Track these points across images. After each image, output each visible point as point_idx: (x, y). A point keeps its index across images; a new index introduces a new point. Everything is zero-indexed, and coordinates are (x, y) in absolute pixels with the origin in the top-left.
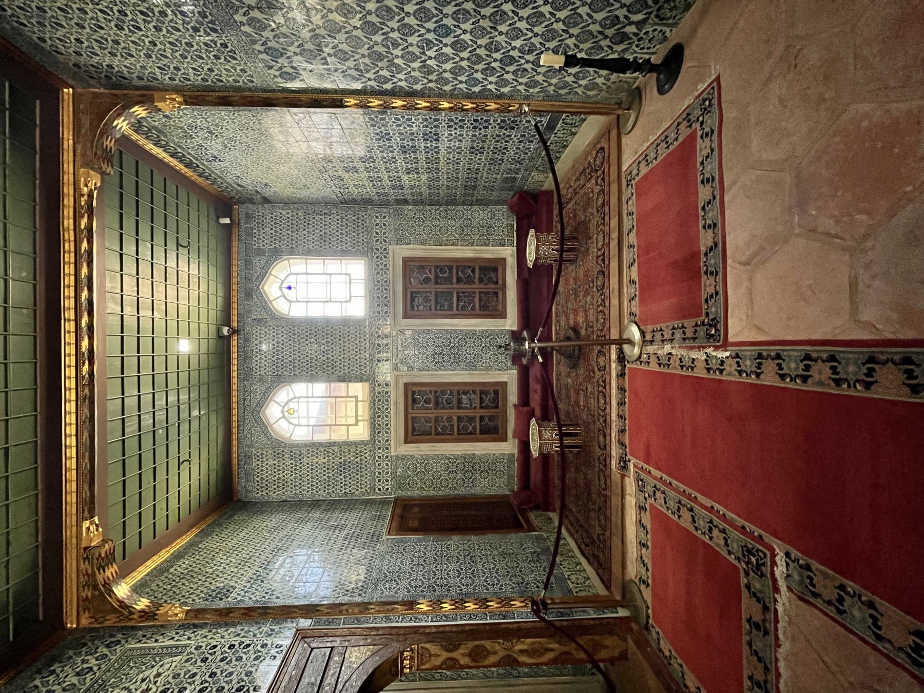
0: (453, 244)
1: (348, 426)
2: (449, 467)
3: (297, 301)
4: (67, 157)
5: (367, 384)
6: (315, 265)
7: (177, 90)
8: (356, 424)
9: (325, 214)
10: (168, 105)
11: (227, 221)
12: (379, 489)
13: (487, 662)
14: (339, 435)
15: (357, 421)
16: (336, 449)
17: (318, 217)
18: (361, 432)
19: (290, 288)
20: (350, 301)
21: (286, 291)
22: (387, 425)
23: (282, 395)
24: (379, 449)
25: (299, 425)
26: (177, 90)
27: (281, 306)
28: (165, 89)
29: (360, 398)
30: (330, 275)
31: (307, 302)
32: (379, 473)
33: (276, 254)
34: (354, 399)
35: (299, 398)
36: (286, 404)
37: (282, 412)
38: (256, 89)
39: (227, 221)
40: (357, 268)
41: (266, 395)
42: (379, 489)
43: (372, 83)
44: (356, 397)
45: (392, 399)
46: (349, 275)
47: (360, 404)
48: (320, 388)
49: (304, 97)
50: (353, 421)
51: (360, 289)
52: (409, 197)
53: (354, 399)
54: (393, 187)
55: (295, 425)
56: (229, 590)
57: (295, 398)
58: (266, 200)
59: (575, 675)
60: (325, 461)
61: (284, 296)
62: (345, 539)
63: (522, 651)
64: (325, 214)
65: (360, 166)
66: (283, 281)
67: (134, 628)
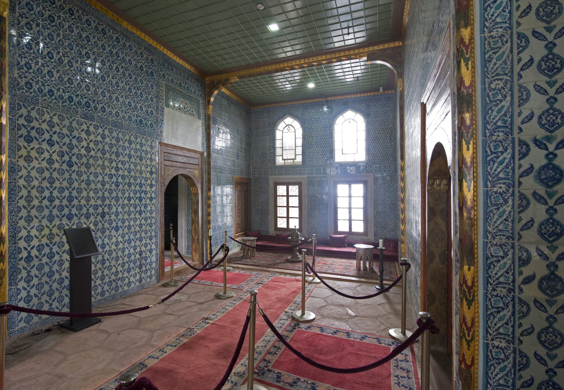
0: (375, 208)
1: (282, 156)
5: (301, 163)
6: (362, 135)
8: (283, 159)
9: (391, 139)
14: (278, 151)
15: (284, 160)
17: (388, 135)
18: (279, 161)
21: (348, 121)
23: (297, 125)
33: (366, 116)
37: (289, 125)
41: (295, 117)
44: (295, 159)
45: (294, 176)
47: (292, 161)
48: (300, 142)
50: (284, 158)
61: (346, 120)
64: (391, 139)
66: (353, 120)
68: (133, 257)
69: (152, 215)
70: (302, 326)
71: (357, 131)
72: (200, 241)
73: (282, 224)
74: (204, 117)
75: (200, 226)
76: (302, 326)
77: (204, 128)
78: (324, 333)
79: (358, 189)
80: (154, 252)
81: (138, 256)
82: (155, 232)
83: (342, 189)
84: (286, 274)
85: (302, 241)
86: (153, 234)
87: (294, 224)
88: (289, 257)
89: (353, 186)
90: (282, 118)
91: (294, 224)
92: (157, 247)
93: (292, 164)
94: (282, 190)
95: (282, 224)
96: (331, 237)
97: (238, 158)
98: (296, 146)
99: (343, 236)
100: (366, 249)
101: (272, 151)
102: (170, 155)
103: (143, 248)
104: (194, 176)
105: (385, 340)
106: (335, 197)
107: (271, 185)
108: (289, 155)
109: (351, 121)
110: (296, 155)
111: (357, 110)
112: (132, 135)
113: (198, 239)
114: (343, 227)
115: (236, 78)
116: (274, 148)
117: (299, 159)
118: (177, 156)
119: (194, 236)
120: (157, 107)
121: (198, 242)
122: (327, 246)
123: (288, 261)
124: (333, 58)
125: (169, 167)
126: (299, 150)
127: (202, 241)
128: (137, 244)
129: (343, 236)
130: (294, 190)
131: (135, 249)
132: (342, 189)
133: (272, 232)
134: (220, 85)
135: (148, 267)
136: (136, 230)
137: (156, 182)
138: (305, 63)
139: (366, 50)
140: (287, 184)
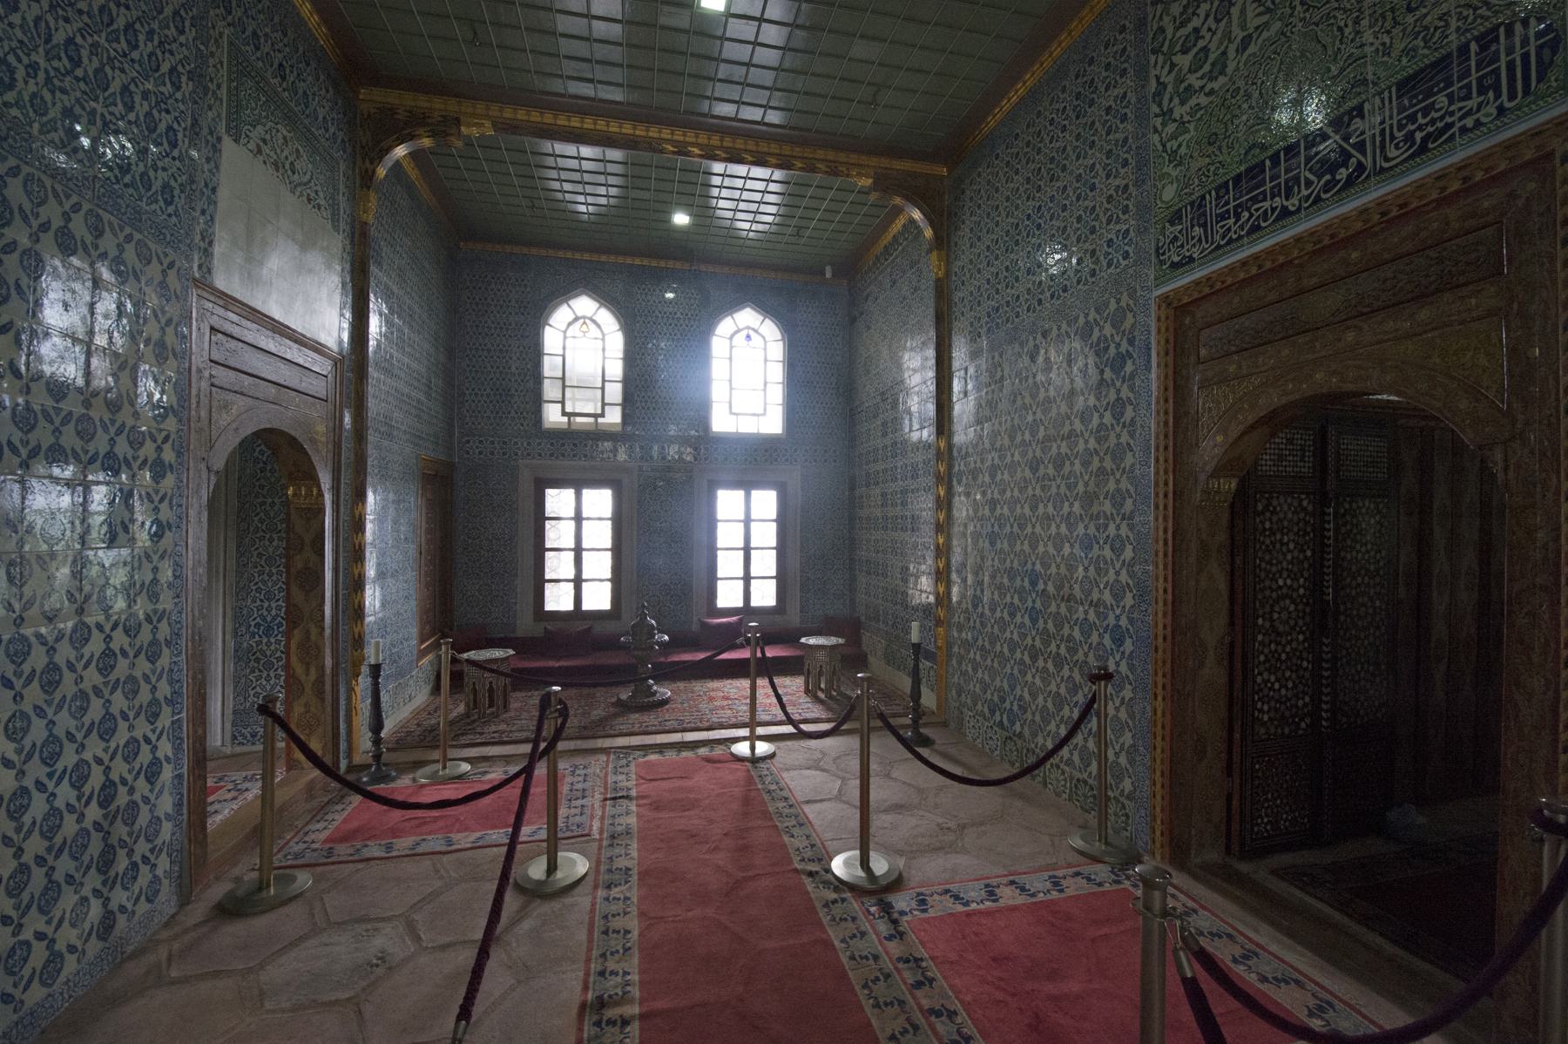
1: (563, 402)
2: (499, 539)
3: (731, 347)
4: (885, 162)
6: (777, 372)
7: (948, 274)
8: (564, 413)
10: (933, 265)
11: (828, 275)
12: (468, 442)
13: (294, 589)
14: (550, 390)
15: (569, 415)
16: (531, 384)
18: (553, 416)
19: (748, 337)
20: (731, 413)
21: (745, 332)
22: (563, 455)
23: (607, 318)
24: (529, 444)
25: (565, 338)
26: (948, 274)
27: (725, 326)
28: (948, 263)
29: (600, 420)
30: (765, 390)
31: (730, 359)
32: (493, 443)
34: (599, 412)
35: (603, 340)
36: (594, 322)
37: (584, 317)
38: (950, 352)
39: (828, 275)
40: (773, 424)
42: (468, 442)
43: (956, 469)
44: (602, 415)
46: (764, 414)
47: (591, 420)
48: (616, 369)
49: (945, 396)
50: (569, 409)
51: (748, 427)
52: (857, 493)
53: (599, 412)
54: (868, 475)
55: (565, 332)
56: (380, 264)
57: (604, 335)
58: (853, 320)
59: (235, 712)
60: (513, 369)
62: (419, 401)
63: (308, 632)
65: (888, 441)
66: (756, 331)
67: (354, 163)
68: (70, 826)
69: (160, 607)
70: (901, 901)
71: (766, 360)
72: (328, 687)
73: (558, 599)
74: (348, 228)
75: (328, 632)
76: (901, 901)
77: (348, 267)
78: (974, 906)
79: (766, 502)
80: (167, 773)
81: (94, 812)
82: (171, 682)
83: (728, 502)
84: (661, 748)
85: (662, 644)
86: (164, 689)
87: (598, 598)
88: (625, 694)
89: (755, 494)
90: (564, 293)
91: (598, 598)
92: (177, 749)
93: (593, 428)
94: (558, 501)
95: (558, 599)
96: (704, 625)
97: (428, 395)
98: (604, 381)
99: (734, 619)
100: (833, 647)
101: (531, 384)
102: (233, 344)
103: (120, 768)
104: (313, 441)
105: (1096, 874)
106: (712, 523)
107: (526, 486)
108: (584, 404)
109: (751, 333)
110: (604, 405)
111: (767, 310)
112: (76, 208)
113: (320, 681)
114: (728, 596)
115: (488, 124)
116: (537, 378)
117: (614, 417)
118: (260, 355)
119: (299, 670)
120: (195, 122)
121: (320, 694)
122: (685, 652)
123: (625, 708)
124: (772, 154)
125: (230, 397)
126: (615, 392)
127: (335, 686)
128: (88, 755)
129: (734, 619)
130: (599, 501)
131: (78, 785)
132: (728, 502)
133: (525, 625)
134: (421, 131)
135: (142, 847)
136: (86, 685)
137: (179, 454)
138: (721, 148)
139: (874, 161)
140: (578, 484)
